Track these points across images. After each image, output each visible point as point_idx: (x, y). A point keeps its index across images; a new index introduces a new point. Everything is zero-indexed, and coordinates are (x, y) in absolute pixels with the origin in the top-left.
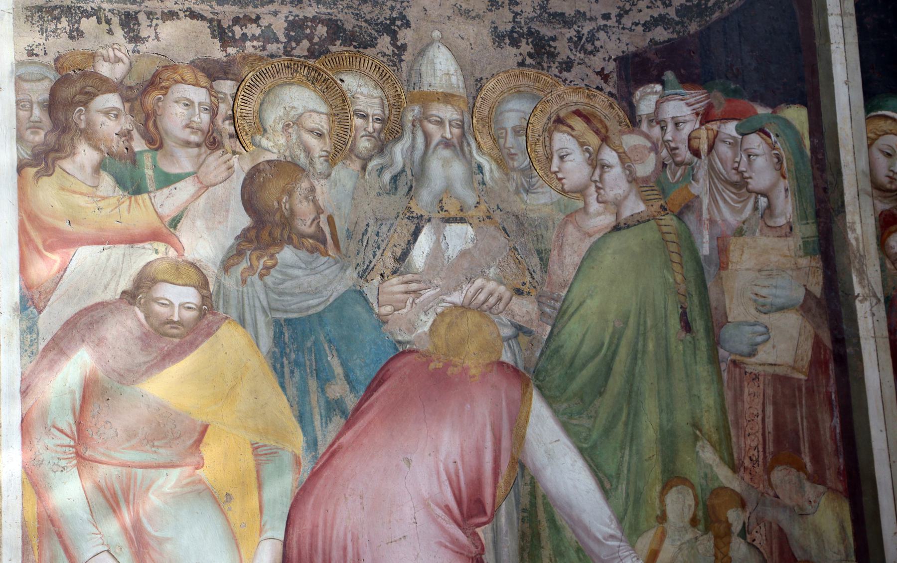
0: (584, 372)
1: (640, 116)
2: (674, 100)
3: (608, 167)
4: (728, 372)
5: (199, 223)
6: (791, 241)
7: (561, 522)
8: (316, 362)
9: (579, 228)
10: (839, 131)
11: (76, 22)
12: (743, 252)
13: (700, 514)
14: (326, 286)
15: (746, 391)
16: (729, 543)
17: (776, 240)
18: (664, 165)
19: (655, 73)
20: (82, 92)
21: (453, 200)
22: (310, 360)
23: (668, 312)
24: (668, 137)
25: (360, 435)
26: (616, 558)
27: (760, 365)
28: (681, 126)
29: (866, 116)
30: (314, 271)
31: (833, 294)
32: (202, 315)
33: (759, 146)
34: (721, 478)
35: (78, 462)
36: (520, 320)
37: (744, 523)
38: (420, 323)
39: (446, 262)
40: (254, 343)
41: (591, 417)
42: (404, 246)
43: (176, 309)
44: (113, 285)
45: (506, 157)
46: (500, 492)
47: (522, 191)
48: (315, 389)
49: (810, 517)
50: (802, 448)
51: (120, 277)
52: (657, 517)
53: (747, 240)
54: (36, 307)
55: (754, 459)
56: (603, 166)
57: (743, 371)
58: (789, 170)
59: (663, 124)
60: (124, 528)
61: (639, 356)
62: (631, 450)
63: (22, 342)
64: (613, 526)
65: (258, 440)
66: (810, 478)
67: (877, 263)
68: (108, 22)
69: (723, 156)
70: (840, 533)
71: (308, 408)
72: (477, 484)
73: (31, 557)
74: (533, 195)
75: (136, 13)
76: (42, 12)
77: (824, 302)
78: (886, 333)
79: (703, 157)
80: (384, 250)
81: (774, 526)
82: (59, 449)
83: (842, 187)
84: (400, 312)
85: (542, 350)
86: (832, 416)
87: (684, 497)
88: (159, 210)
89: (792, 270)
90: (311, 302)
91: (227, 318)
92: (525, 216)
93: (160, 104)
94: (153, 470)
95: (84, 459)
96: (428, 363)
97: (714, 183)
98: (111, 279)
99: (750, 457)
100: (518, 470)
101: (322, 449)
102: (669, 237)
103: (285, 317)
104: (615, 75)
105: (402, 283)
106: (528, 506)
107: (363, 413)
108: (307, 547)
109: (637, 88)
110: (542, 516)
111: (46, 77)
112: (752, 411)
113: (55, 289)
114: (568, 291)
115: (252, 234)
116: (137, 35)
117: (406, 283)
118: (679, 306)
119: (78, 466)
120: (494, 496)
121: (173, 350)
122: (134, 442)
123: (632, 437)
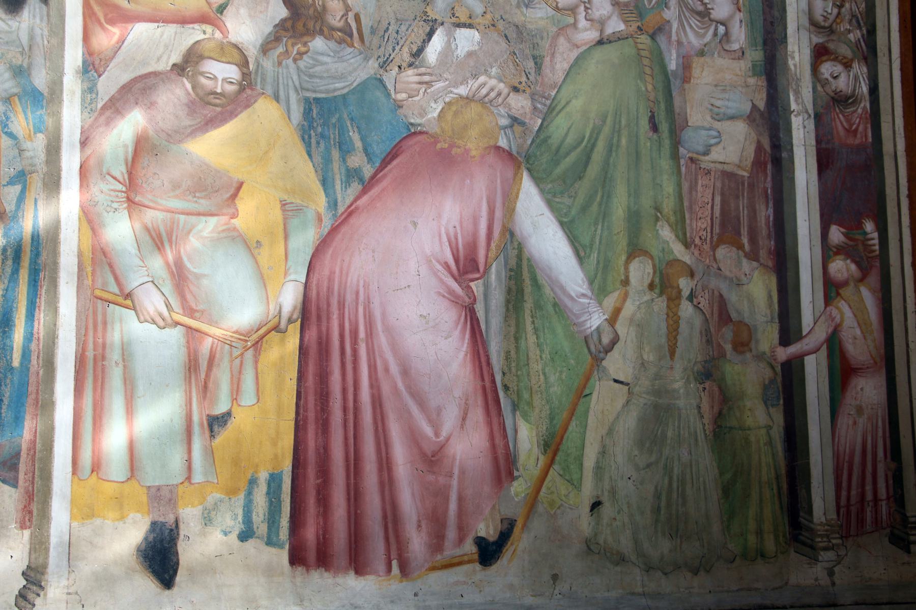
0: (567, 160)
5: (243, 11)
6: (742, 64)
7: (541, 280)
8: (339, 135)
9: (569, 40)
12: (703, 69)
13: (657, 280)
14: (350, 73)
15: (700, 182)
16: (679, 304)
17: (731, 61)
21: (464, 9)
22: (334, 134)
25: (374, 199)
26: (586, 312)
27: (712, 162)
30: (341, 59)
31: (774, 109)
32: (242, 89)
34: (676, 252)
35: (129, 205)
36: (514, 113)
37: (692, 289)
38: (431, 109)
39: (455, 60)
40: (286, 116)
41: (571, 196)
42: (420, 44)
43: (220, 83)
44: (165, 58)
46: (492, 254)
47: (523, 6)
48: (337, 159)
49: (745, 287)
51: (171, 51)
52: (622, 281)
53: (707, 60)
54: (96, 71)
55: (703, 238)
57: (698, 166)
58: (744, 5)
60: (167, 264)
61: (614, 149)
62: (603, 226)
63: (83, 100)
64: (584, 287)
65: (286, 198)
66: (747, 256)
67: (810, 86)
70: (768, 300)
71: (330, 174)
72: (472, 247)
73: (85, 282)
74: (532, 10)
78: (814, 142)
80: (402, 46)
81: (716, 293)
82: (113, 193)
83: (786, 21)
84: (414, 99)
85: (533, 139)
87: (645, 266)
89: (742, 87)
90: (337, 85)
91: (263, 93)
92: (524, 26)
94: (194, 217)
95: (134, 203)
96: (436, 143)
97: (683, 11)
98: (164, 53)
99: (700, 237)
100: (508, 236)
101: (341, 209)
102: (643, 53)
103: (314, 96)
105: (417, 75)
107: (379, 181)
108: (325, 289)
110: (526, 275)
112: (703, 200)
114: (557, 92)
115: (289, 24)
117: (420, 75)
120: (487, 257)
122: (178, 192)
123: (605, 215)
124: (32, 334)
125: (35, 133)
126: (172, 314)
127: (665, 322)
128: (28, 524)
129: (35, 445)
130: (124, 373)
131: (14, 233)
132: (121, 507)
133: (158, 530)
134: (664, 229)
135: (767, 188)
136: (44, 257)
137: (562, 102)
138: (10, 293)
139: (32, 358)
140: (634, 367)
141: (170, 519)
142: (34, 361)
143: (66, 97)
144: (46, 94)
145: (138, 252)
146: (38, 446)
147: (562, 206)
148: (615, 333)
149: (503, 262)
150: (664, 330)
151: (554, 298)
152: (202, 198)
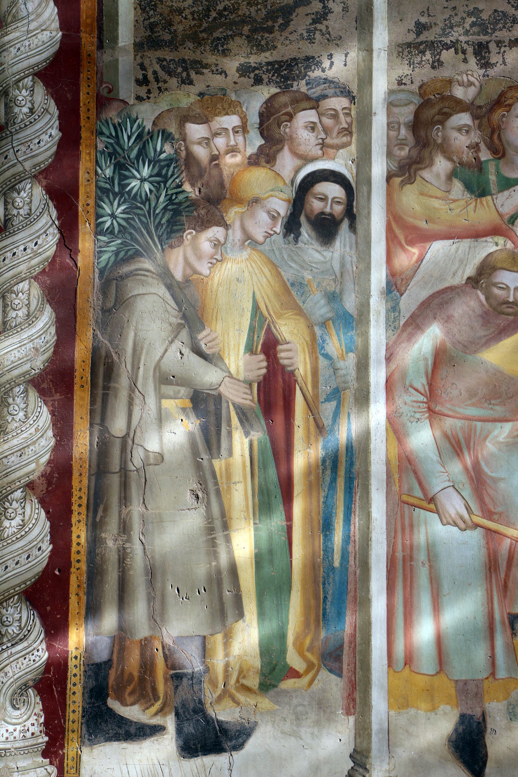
11: (437, 54)
20: (440, 113)
35: (430, 415)
43: (512, 292)
44: (460, 273)
51: (466, 266)
54: (398, 291)
60: (466, 468)
63: (387, 319)
68: (464, 52)
73: (393, 488)
75: (488, 43)
76: (410, 47)
82: (415, 404)
88: (500, 209)
93: (504, 119)
94: (490, 424)
95: (434, 413)
98: (459, 268)
111: (412, 102)
113: (413, 276)
116: (487, 62)
119: (430, 418)
121: (509, 325)
122: (474, 400)
124: (349, 537)
125: (347, 353)
126: (472, 516)
128: (352, 710)
129: (355, 639)
130: (430, 573)
131: (331, 445)
132: (432, 699)
133: (466, 722)
136: (357, 466)
138: (330, 500)
139: (350, 558)
141: (477, 712)
142: (352, 562)
143: (372, 317)
144: (355, 316)
145: (439, 459)
146: (358, 639)
152: (497, 405)
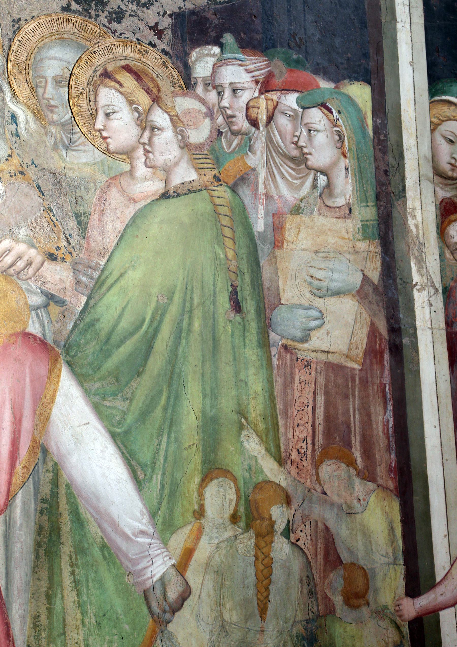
0: (122, 349)
1: (195, 78)
2: (233, 65)
3: (159, 129)
4: (279, 357)
7: (85, 514)
9: (123, 192)
10: (403, 113)
12: (299, 231)
13: (242, 510)
15: (297, 378)
16: (272, 542)
17: (335, 220)
18: (220, 133)
19: (213, 34)
23: (217, 289)
24: (225, 103)
26: (146, 557)
27: (313, 351)
28: (240, 93)
29: (430, 100)
33: (320, 121)
34: (265, 470)
36: (51, 288)
37: (288, 521)
41: (127, 399)
45: (45, 109)
46: (17, 479)
47: (62, 148)
49: (358, 516)
50: (353, 442)
52: (194, 512)
53: (304, 219)
55: (302, 452)
56: (153, 129)
57: (294, 357)
58: (350, 149)
59: (220, 89)
61: (184, 335)
62: (169, 438)
64: (144, 521)
67: (437, 252)
69: (282, 129)
70: (389, 535)
74: (74, 153)
77: (381, 289)
78: (443, 325)
79: (261, 128)
81: (320, 525)
83: (404, 170)
85: (76, 322)
86: (385, 408)
87: (225, 490)
89: (350, 253)
92: (64, 174)
97: (272, 156)
99: (298, 450)
100: (40, 455)
102: (222, 210)
104: (170, 32)
106: (49, 497)
109: (193, 48)
110: (64, 507)
112: (302, 401)
114: (108, 260)
118: (230, 284)
127: (253, 567)
134: (251, 440)
135: (385, 384)
137: (114, 273)
140: (211, 631)
147: (114, 412)
148: (185, 584)
149: (32, 490)
150: (251, 579)
151: (102, 538)
